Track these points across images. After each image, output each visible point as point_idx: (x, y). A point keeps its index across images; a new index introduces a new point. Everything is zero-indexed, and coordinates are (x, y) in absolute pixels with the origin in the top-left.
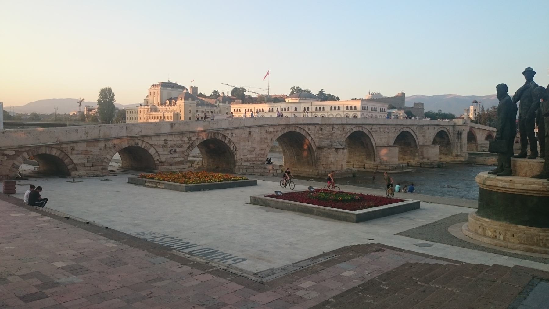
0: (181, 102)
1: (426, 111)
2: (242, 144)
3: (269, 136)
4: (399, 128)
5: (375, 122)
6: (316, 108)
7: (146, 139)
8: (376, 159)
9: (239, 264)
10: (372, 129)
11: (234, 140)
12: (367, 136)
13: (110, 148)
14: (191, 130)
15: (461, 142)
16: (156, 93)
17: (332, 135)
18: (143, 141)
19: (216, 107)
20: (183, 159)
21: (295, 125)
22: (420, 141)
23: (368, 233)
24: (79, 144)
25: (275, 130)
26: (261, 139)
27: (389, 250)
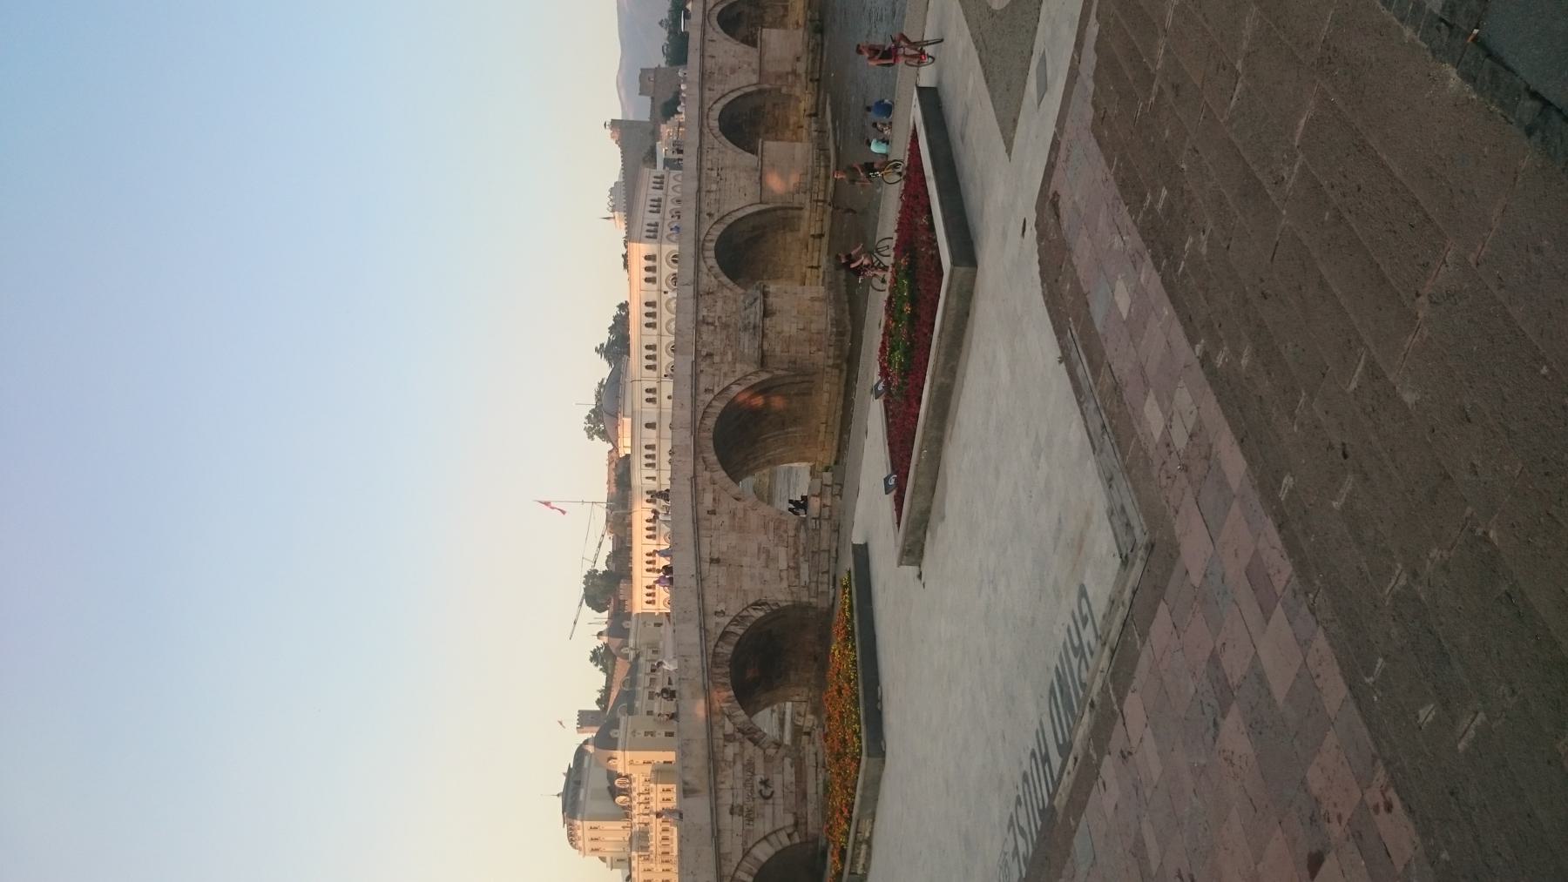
0: (622, 761)
1: (662, 62)
2: (747, 584)
3: (727, 504)
4: (709, 138)
5: (693, 205)
6: (648, 367)
9: (1094, 608)
10: (710, 215)
11: (734, 608)
14: (704, 736)
17: (726, 326)
19: (637, 656)
20: (787, 761)
21: (696, 431)
22: (745, 80)
23: (1004, 235)
25: (710, 488)
26: (733, 528)
27: (1054, 179)
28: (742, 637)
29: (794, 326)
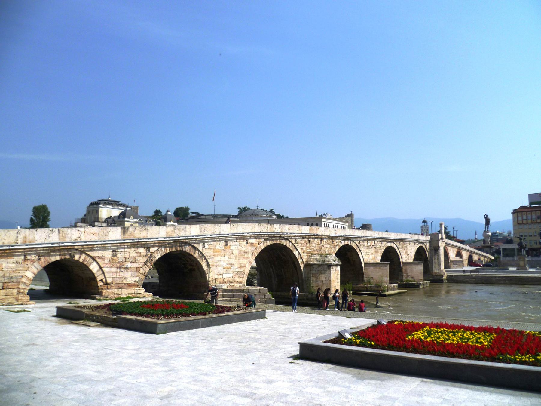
11: (206, 253)
12: (356, 251)
26: (240, 252)
29: (323, 279)
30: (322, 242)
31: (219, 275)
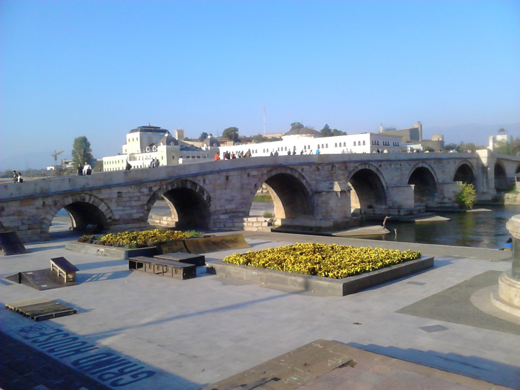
2: (218, 192)
4: (413, 163)
7: (94, 193)
8: (388, 202)
10: (380, 166)
12: (376, 174)
13: (50, 206)
15: (487, 178)
16: (135, 139)
18: (91, 195)
20: (142, 215)
24: (10, 204)
26: (242, 185)
28: (195, 191)
30: (334, 169)
31: (221, 207)
